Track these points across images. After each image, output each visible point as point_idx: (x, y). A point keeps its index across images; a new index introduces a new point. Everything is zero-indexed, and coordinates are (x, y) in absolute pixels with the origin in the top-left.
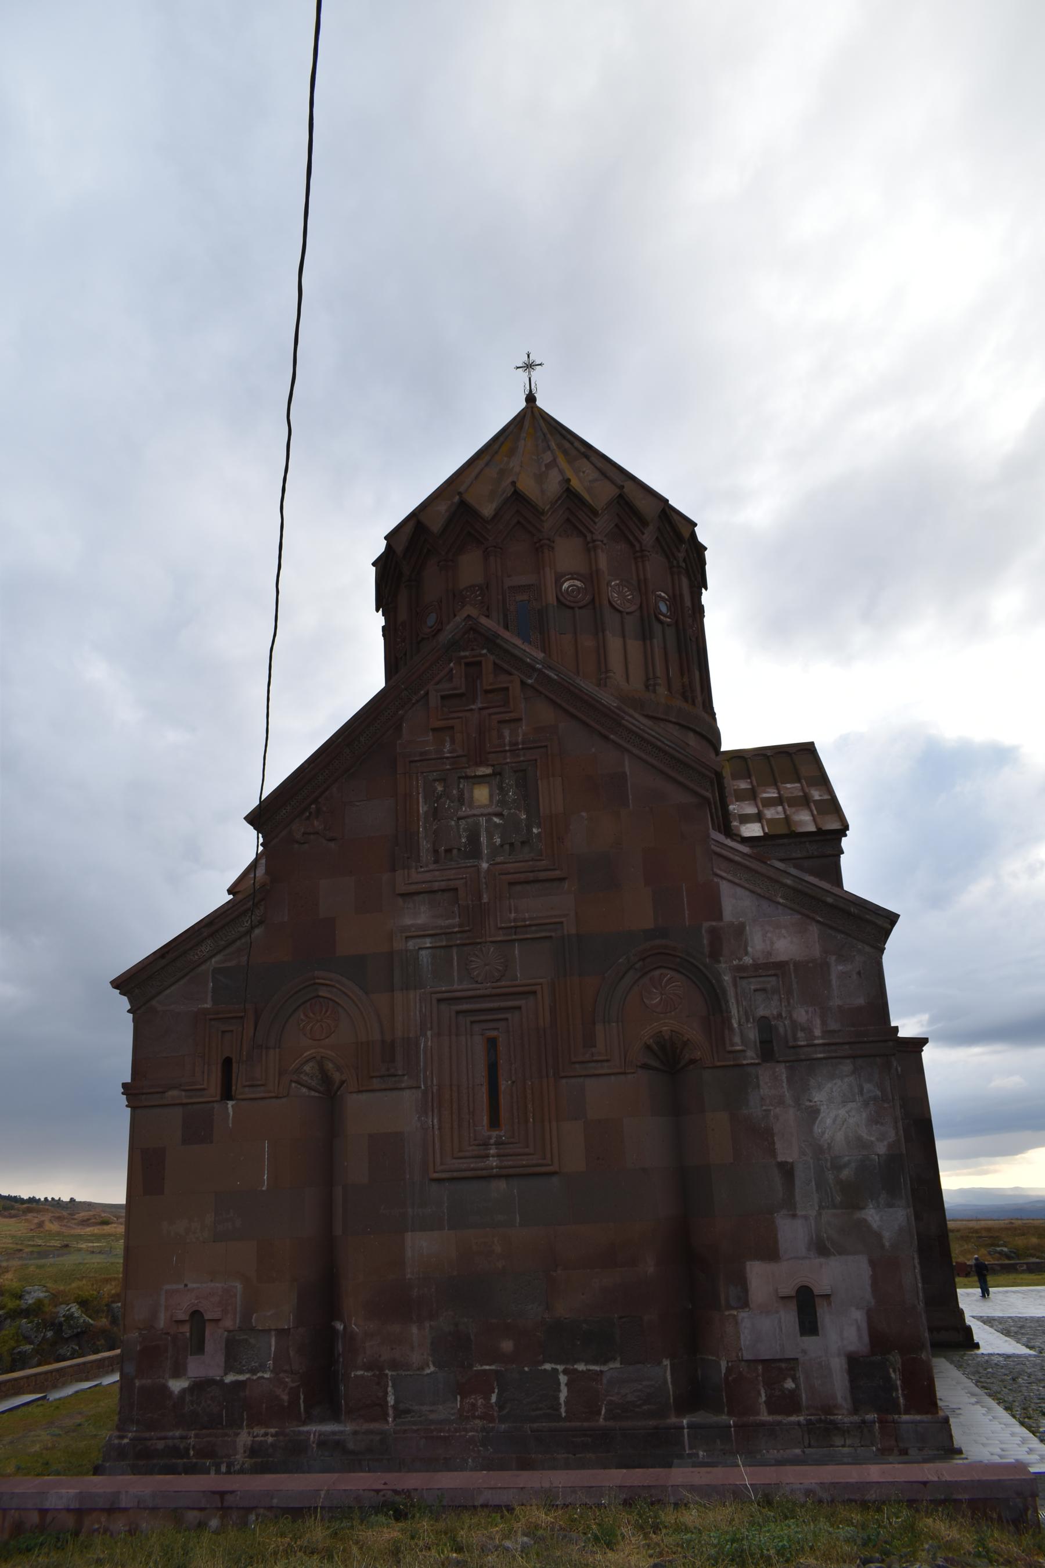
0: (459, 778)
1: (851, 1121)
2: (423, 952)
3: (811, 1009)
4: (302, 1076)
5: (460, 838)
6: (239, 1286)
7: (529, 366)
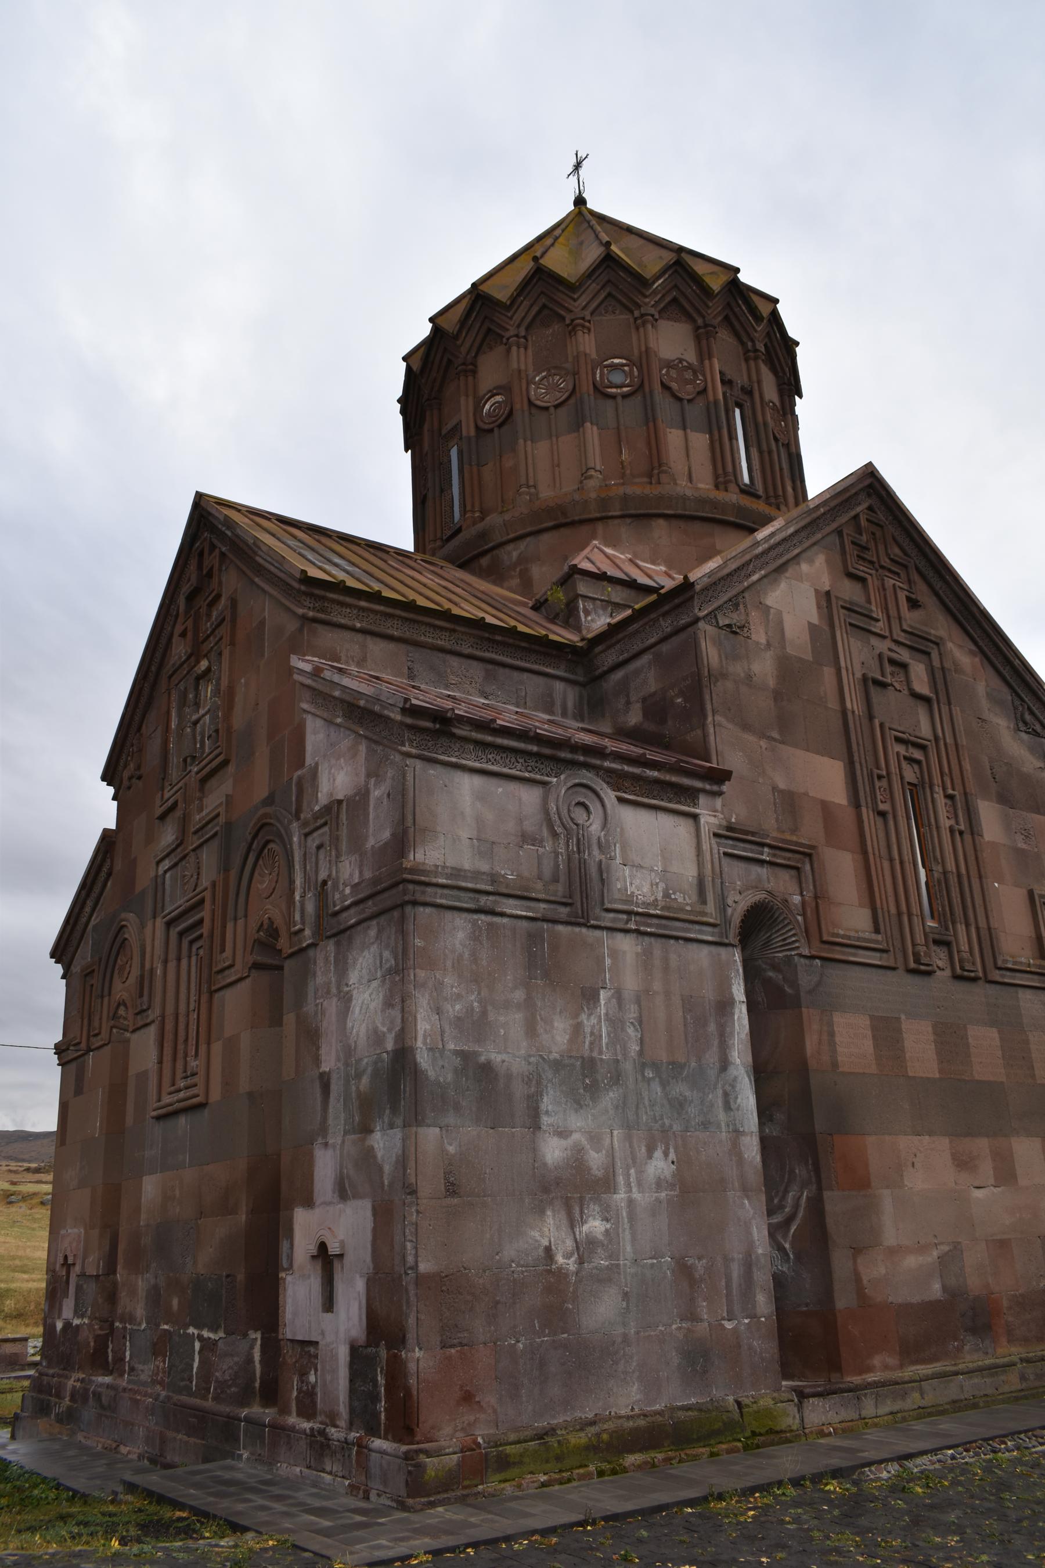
0: (198, 679)
1: (372, 1006)
2: (168, 875)
3: (353, 859)
4: (121, 1020)
5: (195, 744)
6: (82, 1230)
7: (578, 166)
